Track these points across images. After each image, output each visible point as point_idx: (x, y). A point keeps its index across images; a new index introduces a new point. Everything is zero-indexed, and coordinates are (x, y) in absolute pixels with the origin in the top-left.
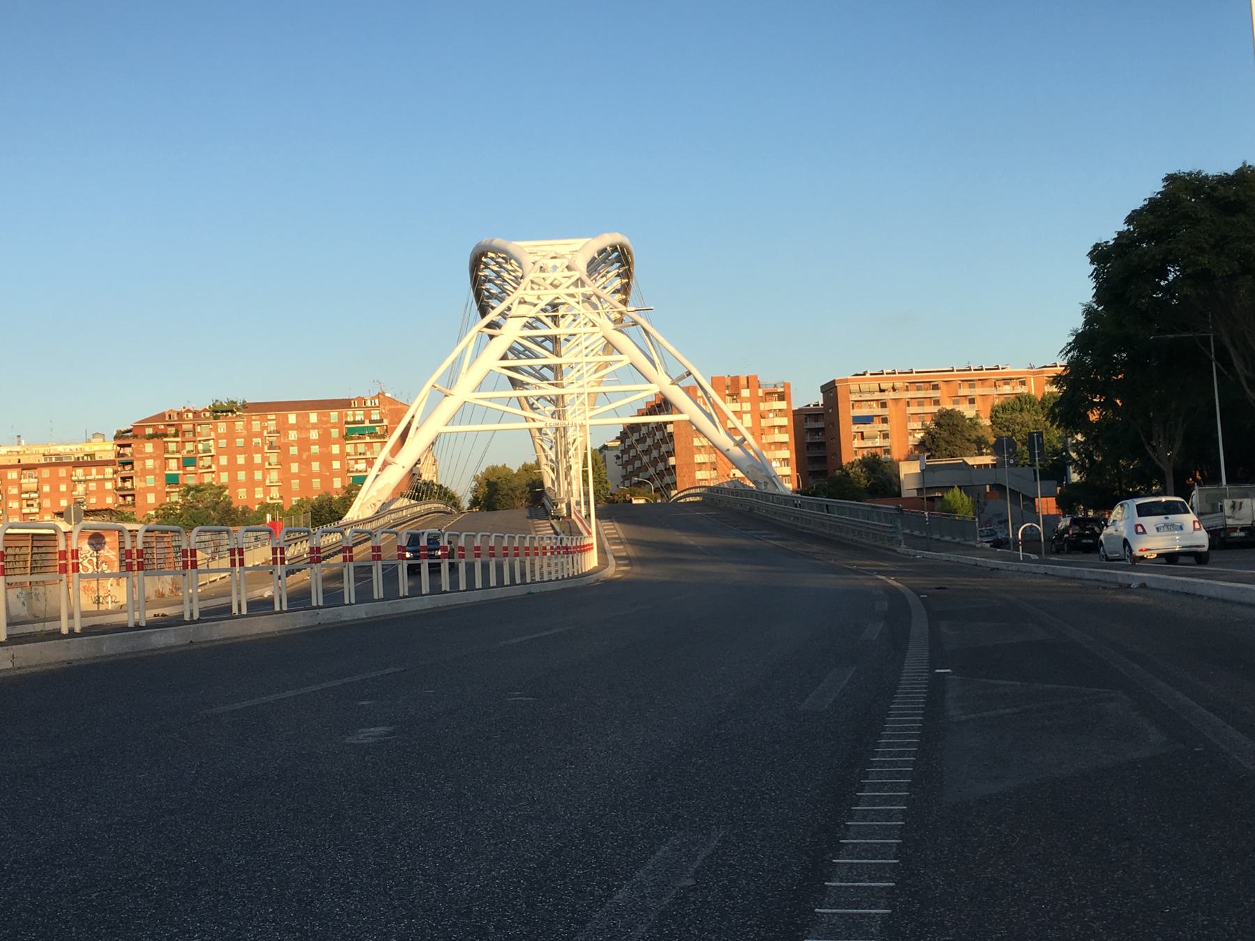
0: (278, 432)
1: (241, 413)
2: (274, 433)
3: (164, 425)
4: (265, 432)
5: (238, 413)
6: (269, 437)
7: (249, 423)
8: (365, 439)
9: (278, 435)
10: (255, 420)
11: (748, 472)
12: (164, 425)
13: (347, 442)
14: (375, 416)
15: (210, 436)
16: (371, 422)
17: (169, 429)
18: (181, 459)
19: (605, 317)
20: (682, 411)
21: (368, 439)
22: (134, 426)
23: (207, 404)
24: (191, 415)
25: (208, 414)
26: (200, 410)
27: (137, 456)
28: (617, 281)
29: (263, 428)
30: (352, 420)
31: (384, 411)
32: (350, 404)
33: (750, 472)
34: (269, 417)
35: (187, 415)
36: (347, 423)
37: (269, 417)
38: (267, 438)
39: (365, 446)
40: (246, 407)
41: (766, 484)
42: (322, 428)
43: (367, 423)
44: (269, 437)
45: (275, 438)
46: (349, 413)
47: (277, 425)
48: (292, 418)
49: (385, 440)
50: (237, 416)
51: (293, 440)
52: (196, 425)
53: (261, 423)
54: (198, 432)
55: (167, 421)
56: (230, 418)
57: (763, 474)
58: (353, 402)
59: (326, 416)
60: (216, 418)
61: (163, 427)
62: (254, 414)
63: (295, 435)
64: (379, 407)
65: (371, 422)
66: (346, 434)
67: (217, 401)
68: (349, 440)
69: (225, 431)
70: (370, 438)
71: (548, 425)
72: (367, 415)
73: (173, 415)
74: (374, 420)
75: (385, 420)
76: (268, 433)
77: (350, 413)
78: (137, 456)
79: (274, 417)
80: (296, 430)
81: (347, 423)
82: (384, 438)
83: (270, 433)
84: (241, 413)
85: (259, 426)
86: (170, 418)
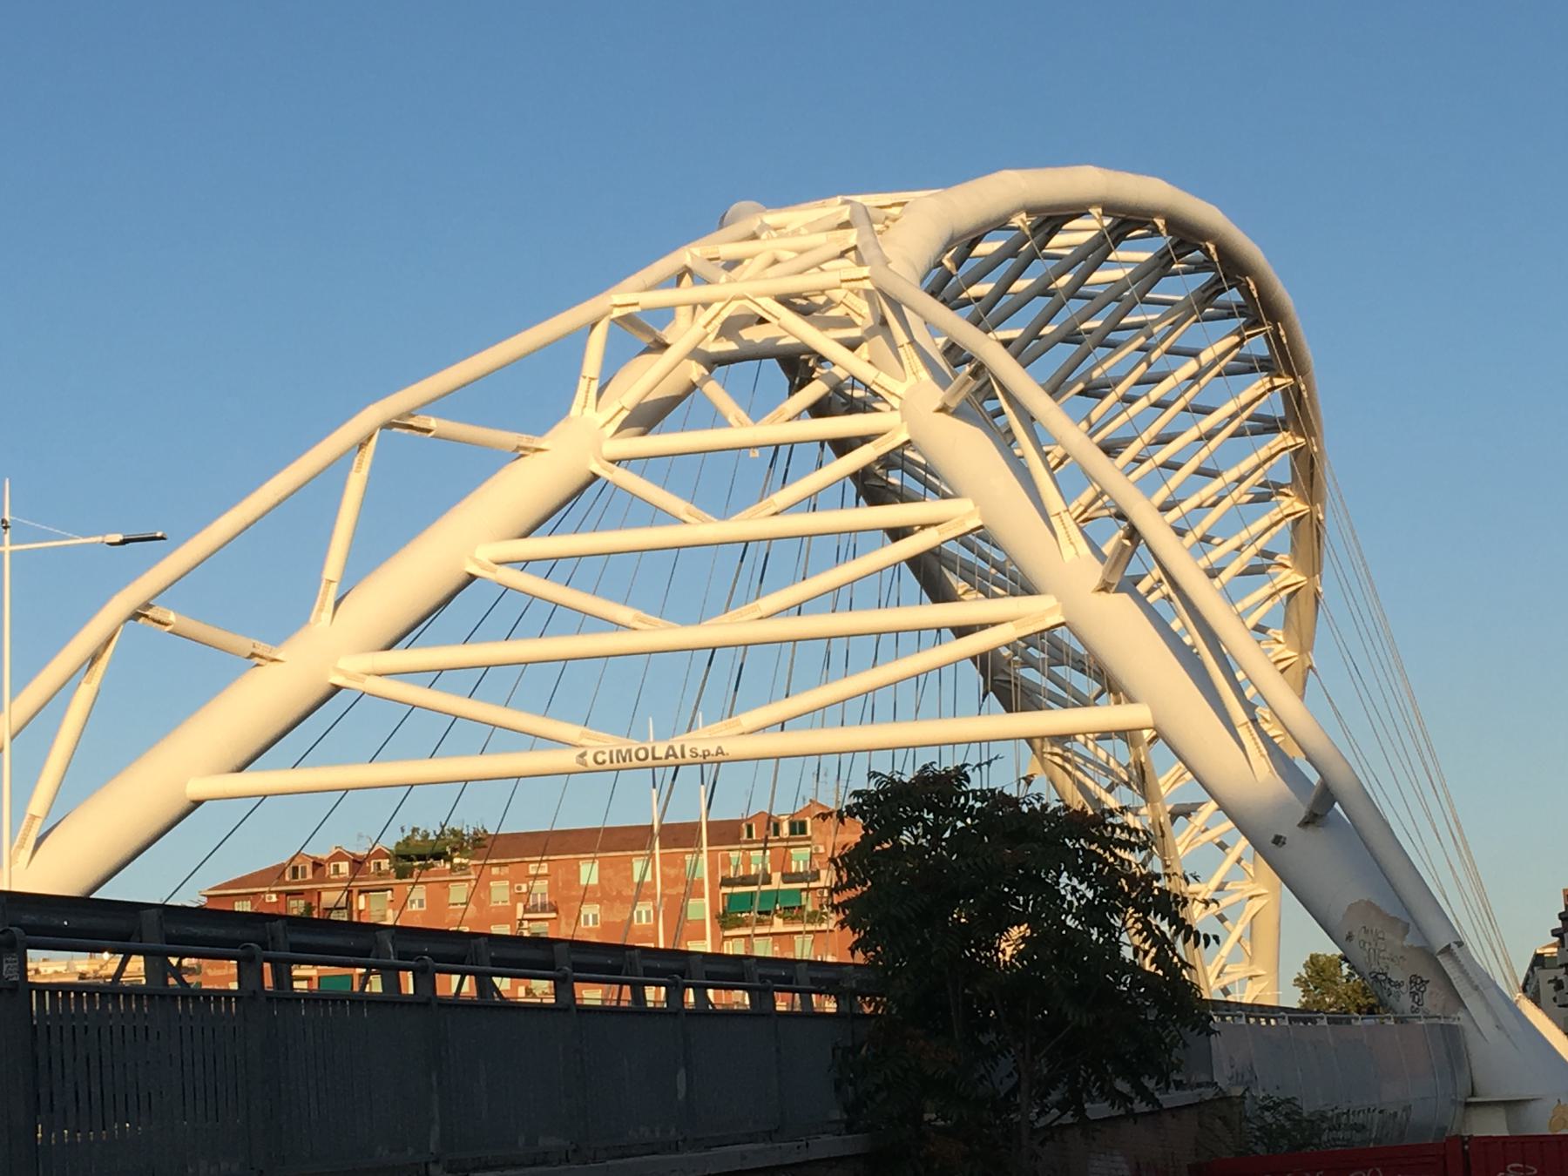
0: (556, 910)
1: (464, 861)
2: (543, 909)
3: (278, 893)
4: (520, 907)
5: (456, 861)
6: (530, 920)
7: (481, 884)
8: (772, 924)
9: (553, 915)
10: (499, 878)
11: (1349, 937)
12: (278, 893)
13: (727, 933)
14: (799, 862)
15: (385, 920)
16: (788, 877)
17: (293, 903)
18: (315, 981)
19: (924, 375)
20: (1134, 693)
21: (779, 925)
22: (209, 897)
23: (390, 842)
24: (344, 867)
25: (385, 864)
26: (362, 852)
27: (210, 972)
28: (1259, 383)
29: (517, 897)
30: (741, 873)
31: (822, 850)
32: (739, 835)
33: (1359, 935)
34: (532, 870)
35: (337, 867)
36: (727, 882)
37: (532, 870)
38: (526, 924)
39: (773, 942)
40: (482, 845)
41: (1417, 983)
42: (670, 896)
43: (777, 883)
44: (530, 920)
45: (547, 924)
46: (732, 854)
47: (552, 888)
48: (589, 873)
49: (824, 927)
50: (453, 869)
51: (589, 930)
52: (355, 891)
53: (511, 886)
54: (360, 911)
55: (287, 884)
56: (443, 873)
57: (1408, 941)
58: (744, 825)
59: (674, 866)
60: (402, 874)
61: (274, 898)
62: (495, 861)
63: (595, 917)
64: (809, 839)
65: (788, 877)
66: (724, 911)
67: (415, 830)
68: (730, 928)
69: (425, 908)
70: (784, 923)
71: (589, 759)
72: (783, 862)
73: (304, 869)
74: (798, 873)
75: (823, 873)
76: (526, 911)
77: (734, 855)
78: (210, 972)
79: (544, 869)
80: (599, 901)
81: (727, 882)
82: (822, 921)
83: (534, 909)
84: (464, 861)
85: (507, 892)
86: (295, 875)
